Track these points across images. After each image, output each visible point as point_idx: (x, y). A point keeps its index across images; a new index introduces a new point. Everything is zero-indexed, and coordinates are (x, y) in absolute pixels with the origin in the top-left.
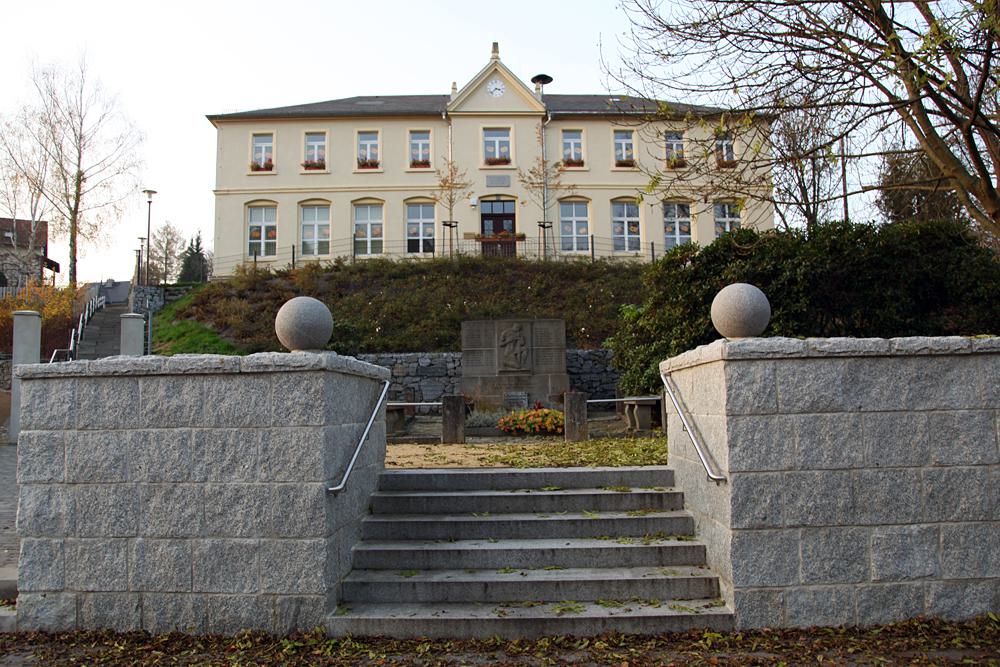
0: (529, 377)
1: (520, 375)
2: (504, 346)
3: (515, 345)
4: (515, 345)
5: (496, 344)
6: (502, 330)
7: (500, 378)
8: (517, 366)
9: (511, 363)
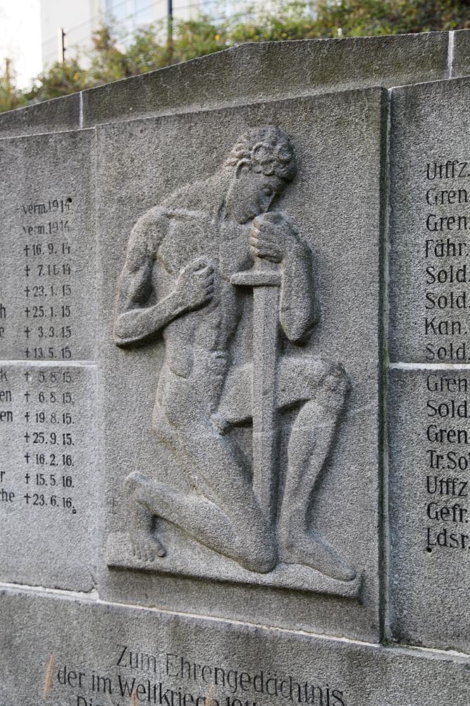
0: (356, 658)
1: (274, 624)
2: (151, 341)
3: (229, 339)
4: (229, 339)
5: (104, 320)
6: (140, 204)
7: (114, 627)
8: (247, 539)
9: (197, 503)
